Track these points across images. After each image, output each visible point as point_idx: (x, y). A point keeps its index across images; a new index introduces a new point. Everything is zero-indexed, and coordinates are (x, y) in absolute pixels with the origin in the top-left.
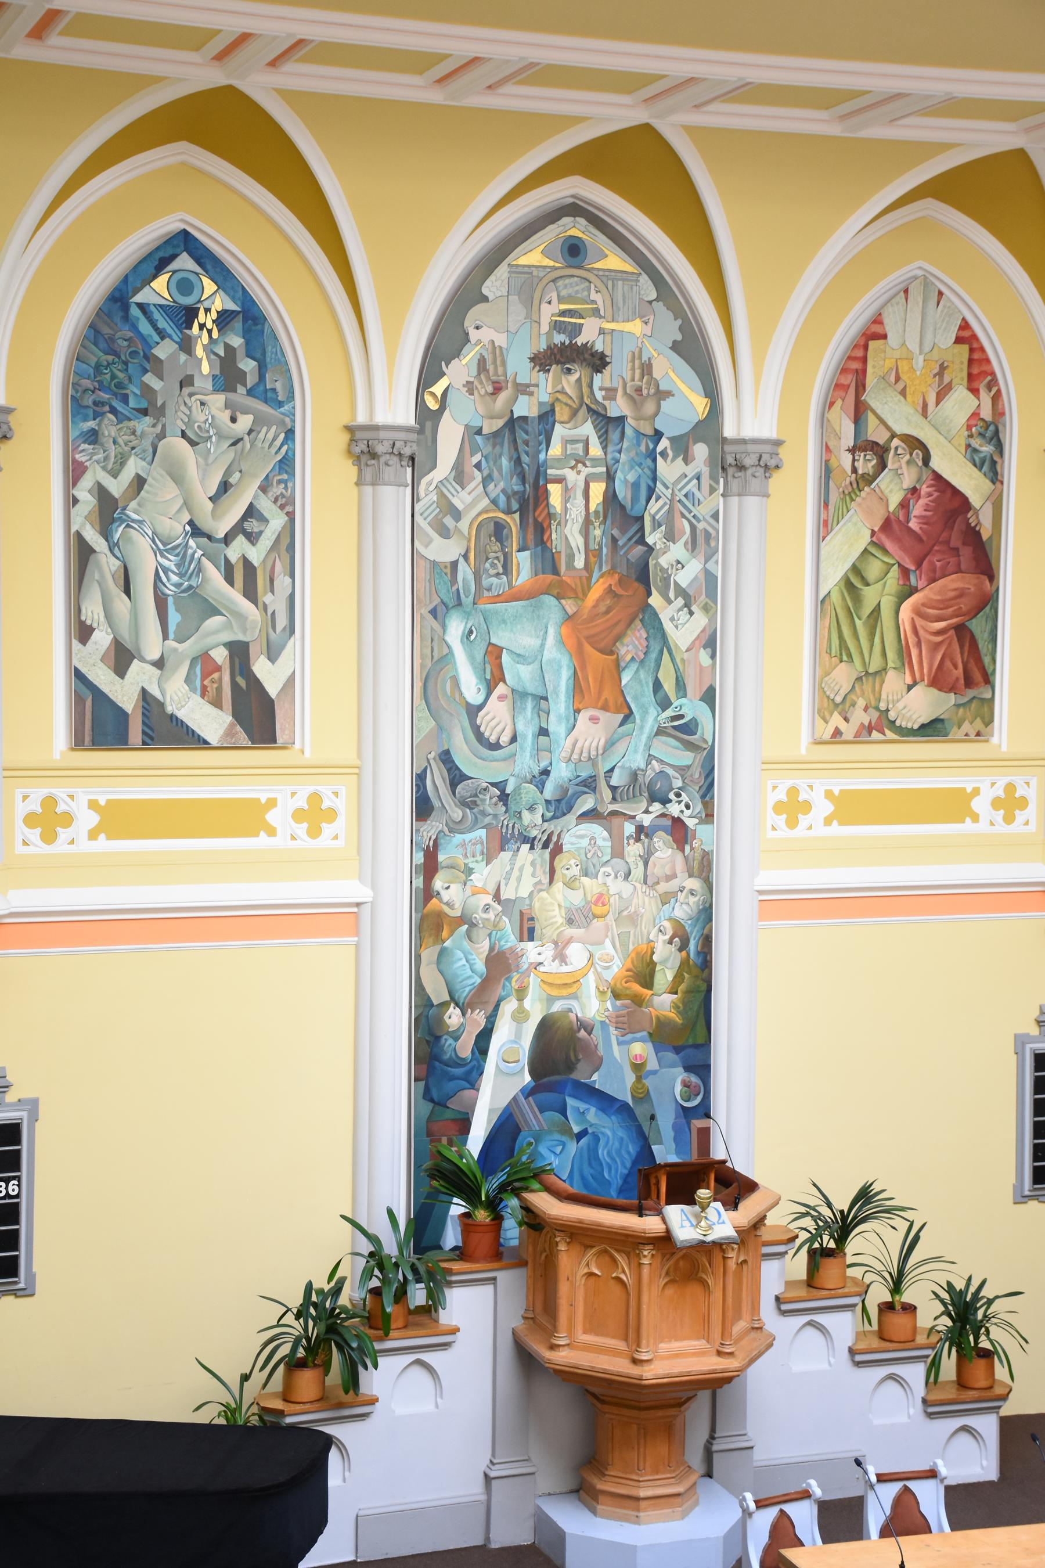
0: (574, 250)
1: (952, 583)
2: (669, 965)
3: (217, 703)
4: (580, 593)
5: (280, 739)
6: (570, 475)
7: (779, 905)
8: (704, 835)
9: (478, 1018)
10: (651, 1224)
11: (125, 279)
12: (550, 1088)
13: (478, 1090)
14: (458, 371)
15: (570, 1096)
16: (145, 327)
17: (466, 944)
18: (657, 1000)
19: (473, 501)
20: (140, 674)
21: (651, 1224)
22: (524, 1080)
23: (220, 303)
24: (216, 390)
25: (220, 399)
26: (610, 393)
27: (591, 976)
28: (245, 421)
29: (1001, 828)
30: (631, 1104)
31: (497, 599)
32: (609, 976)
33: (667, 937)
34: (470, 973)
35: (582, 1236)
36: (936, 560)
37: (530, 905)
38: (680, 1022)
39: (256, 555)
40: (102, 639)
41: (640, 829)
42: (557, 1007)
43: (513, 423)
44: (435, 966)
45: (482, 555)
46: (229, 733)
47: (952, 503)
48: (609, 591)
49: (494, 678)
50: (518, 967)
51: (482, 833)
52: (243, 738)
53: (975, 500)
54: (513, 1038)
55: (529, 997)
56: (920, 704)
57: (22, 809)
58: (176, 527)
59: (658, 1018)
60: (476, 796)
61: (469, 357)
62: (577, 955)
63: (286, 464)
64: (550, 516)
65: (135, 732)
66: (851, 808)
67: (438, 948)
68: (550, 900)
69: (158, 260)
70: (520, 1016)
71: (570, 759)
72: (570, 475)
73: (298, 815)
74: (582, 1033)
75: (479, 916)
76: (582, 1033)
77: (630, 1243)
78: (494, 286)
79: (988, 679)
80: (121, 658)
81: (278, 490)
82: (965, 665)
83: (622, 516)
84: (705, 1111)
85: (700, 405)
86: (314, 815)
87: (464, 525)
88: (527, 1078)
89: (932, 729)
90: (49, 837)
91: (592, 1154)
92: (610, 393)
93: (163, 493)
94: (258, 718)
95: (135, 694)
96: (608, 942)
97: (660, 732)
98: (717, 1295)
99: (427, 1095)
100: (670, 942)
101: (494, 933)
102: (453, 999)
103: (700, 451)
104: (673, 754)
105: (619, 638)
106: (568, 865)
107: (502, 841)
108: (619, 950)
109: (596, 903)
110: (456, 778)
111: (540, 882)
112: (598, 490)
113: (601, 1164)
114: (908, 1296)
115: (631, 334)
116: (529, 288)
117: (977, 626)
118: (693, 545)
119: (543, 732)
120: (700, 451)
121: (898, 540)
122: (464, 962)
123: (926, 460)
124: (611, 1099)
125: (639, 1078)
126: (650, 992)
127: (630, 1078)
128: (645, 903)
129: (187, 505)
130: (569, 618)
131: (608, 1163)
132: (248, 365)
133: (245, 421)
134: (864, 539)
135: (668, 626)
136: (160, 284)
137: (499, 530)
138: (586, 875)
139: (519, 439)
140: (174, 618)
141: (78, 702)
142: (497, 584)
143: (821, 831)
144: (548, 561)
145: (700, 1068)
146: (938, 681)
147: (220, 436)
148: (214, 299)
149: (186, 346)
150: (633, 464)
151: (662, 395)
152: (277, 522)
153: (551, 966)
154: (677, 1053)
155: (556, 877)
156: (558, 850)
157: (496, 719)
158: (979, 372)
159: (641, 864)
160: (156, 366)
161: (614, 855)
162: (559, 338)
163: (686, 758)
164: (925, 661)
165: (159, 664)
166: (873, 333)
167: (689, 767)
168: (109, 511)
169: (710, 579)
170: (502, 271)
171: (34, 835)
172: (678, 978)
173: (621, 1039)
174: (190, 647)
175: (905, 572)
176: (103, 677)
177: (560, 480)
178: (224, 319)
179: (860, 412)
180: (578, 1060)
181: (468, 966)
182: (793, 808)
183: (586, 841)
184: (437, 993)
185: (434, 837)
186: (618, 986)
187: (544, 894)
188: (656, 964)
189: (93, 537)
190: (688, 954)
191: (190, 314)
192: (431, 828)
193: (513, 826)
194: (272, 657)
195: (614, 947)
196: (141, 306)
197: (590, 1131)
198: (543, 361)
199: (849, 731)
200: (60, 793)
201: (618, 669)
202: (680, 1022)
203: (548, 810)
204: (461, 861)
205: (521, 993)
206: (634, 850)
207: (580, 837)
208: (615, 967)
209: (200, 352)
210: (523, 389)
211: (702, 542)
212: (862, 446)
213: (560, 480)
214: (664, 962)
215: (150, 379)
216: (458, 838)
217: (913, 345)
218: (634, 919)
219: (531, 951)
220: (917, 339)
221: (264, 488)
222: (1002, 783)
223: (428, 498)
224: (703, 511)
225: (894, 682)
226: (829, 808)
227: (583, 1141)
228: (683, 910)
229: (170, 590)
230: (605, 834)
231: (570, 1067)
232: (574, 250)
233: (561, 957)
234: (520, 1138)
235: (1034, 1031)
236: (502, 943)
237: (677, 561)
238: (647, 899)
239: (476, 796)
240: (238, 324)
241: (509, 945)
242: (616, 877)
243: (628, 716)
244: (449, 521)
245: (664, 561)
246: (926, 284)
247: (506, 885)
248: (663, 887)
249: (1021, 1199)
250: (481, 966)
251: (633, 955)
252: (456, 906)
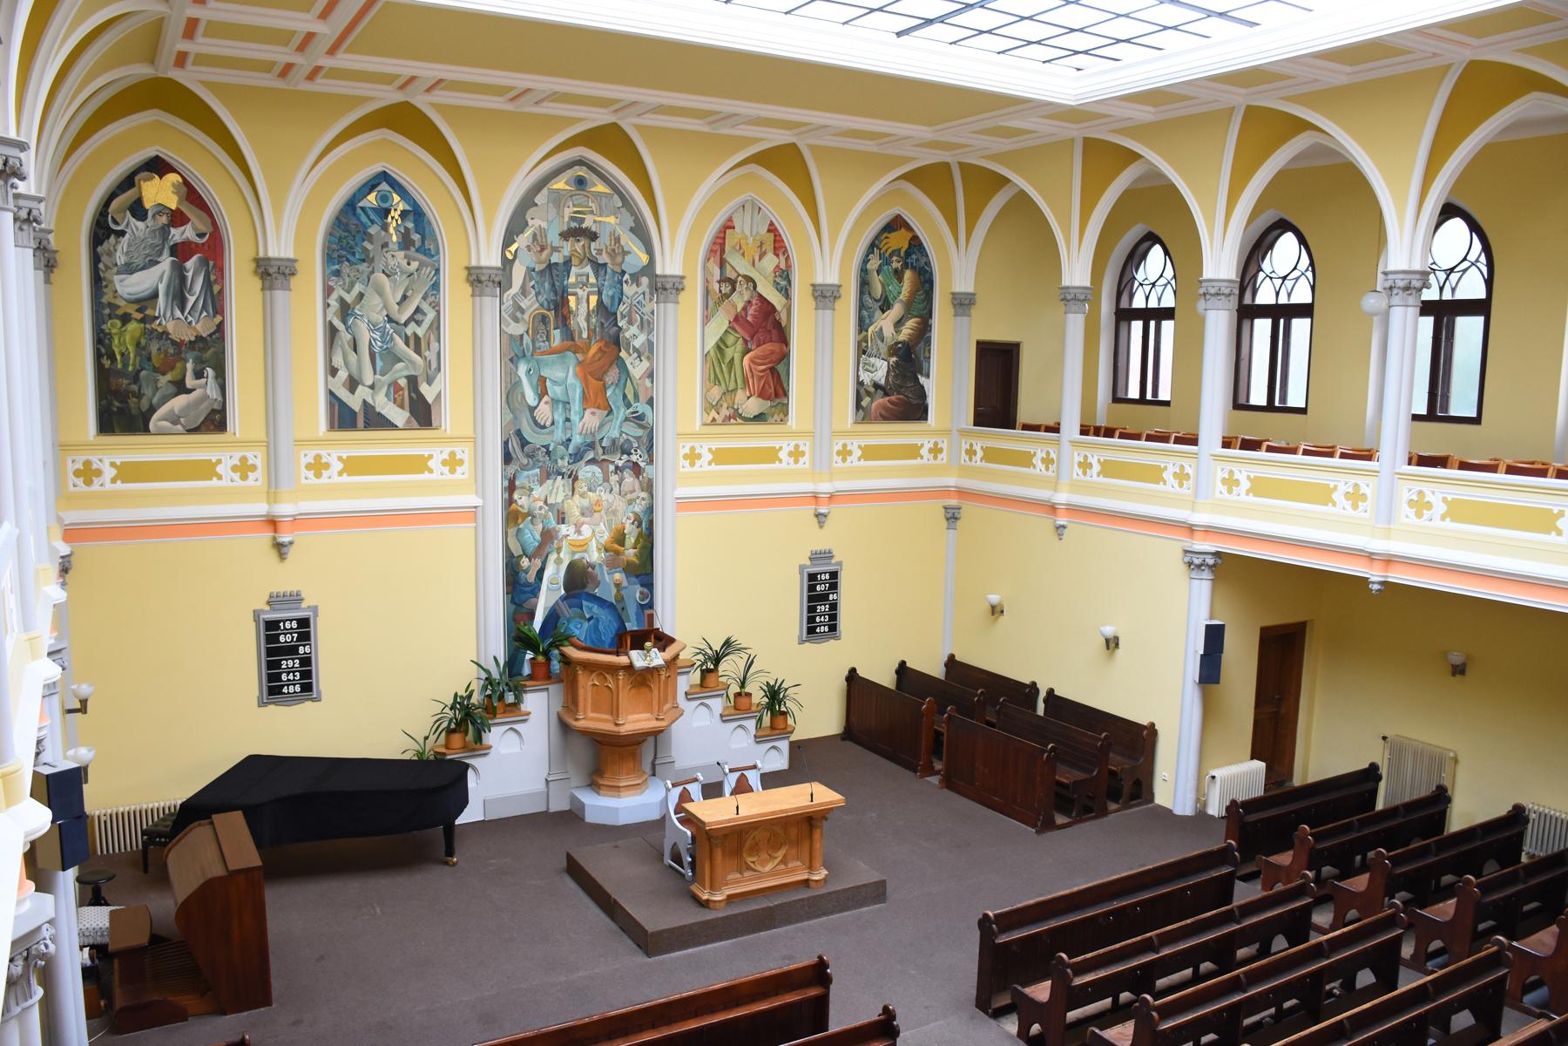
0: (580, 182)
1: (768, 347)
3: (402, 407)
4: (583, 349)
5: (434, 424)
6: (580, 291)
7: (687, 505)
8: (649, 471)
10: (623, 660)
11: (354, 195)
12: (574, 596)
14: (523, 240)
16: (364, 218)
19: (530, 304)
20: (362, 392)
21: (623, 660)
23: (401, 207)
24: (400, 249)
25: (402, 253)
26: (600, 252)
28: (415, 265)
29: (792, 466)
31: (542, 354)
32: (602, 541)
35: (589, 666)
36: (760, 336)
39: (420, 332)
40: (343, 374)
41: (617, 468)
42: (577, 556)
43: (551, 266)
45: (536, 332)
46: (408, 422)
47: (767, 308)
48: (600, 349)
49: (542, 392)
52: (415, 424)
53: (779, 307)
56: (753, 406)
57: (304, 461)
58: (380, 318)
61: (528, 233)
62: (586, 530)
63: (436, 286)
64: (570, 312)
65: (360, 421)
66: (720, 457)
69: (371, 185)
70: (559, 561)
72: (580, 291)
73: (444, 463)
75: (537, 512)
77: (613, 669)
78: (541, 199)
79: (786, 394)
80: (353, 384)
81: (431, 299)
82: (774, 387)
83: (606, 312)
84: (651, 605)
85: (644, 258)
86: (452, 463)
87: (526, 317)
89: (760, 418)
90: (318, 475)
91: (596, 629)
92: (600, 252)
93: (373, 301)
94: (423, 414)
95: (360, 402)
97: (626, 419)
98: (656, 692)
99: (513, 601)
103: (645, 280)
104: (633, 431)
105: (605, 373)
106: (582, 486)
107: (547, 475)
110: (524, 443)
112: (594, 299)
114: (747, 690)
115: (609, 223)
116: (558, 199)
117: (780, 368)
118: (641, 327)
119: (568, 420)
120: (645, 280)
121: (742, 326)
123: (755, 287)
127: (614, 591)
128: (620, 504)
129: (385, 307)
130: (580, 363)
132: (416, 237)
133: (415, 265)
134: (726, 325)
135: (630, 367)
136: (372, 197)
137: (544, 319)
139: (554, 274)
140: (379, 364)
141: (331, 407)
142: (543, 346)
143: (706, 468)
144: (569, 335)
145: (648, 584)
146: (762, 395)
147: (402, 272)
148: (398, 204)
149: (385, 227)
150: (611, 287)
151: (625, 253)
152: (431, 315)
153: (573, 536)
156: (576, 479)
157: (544, 412)
158: (779, 246)
160: (370, 238)
162: (574, 225)
163: (639, 432)
164: (755, 384)
165: (372, 387)
166: (728, 226)
168: (345, 310)
169: (650, 344)
170: (545, 191)
171: (311, 474)
172: (637, 541)
174: (387, 378)
175: (745, 341)
176: (343, 394)
177: (575, 294)
178: (404, 214)
179: (722, 264)
182: (693, 457)
184: (517, 551)
189: (337, 323)
191: (388, 211)
192: (511, 469)
194: (430, 383)
196: (363, 209)
198: (565, 235)
199: (719, 419)
200: (323, 453)
201: (605, 388)
205: (559, 550)
206: (614, 478)
207: (587, 472)
208: (606, 537)
209: (391, 230)
210: (555, 249)
211: (646, 325)
212: (724, 280)
213: (575, 294)
215: (367, 244)
217: (748, 233)
218: (614, 513)
219: (563, 529)
220: (748, 230)
221: (424, 298)
222: (793, 444)
223: (508, 303)
224: (646, 310)
225: (741, 395)
226: (710, 457)
228: (639, 508)
229: (377, 350)
231: (584, 586)
232: (580, 182)
233: (579, 532)
235: (808, 563)
237: (634, 335)
240: (411, 217)
243: (610, 412)
244: (518, 314)
245: (627, 335)
246: (753, 204)
248: (629, 496)
249: (802, 642)
250: (538, 537)
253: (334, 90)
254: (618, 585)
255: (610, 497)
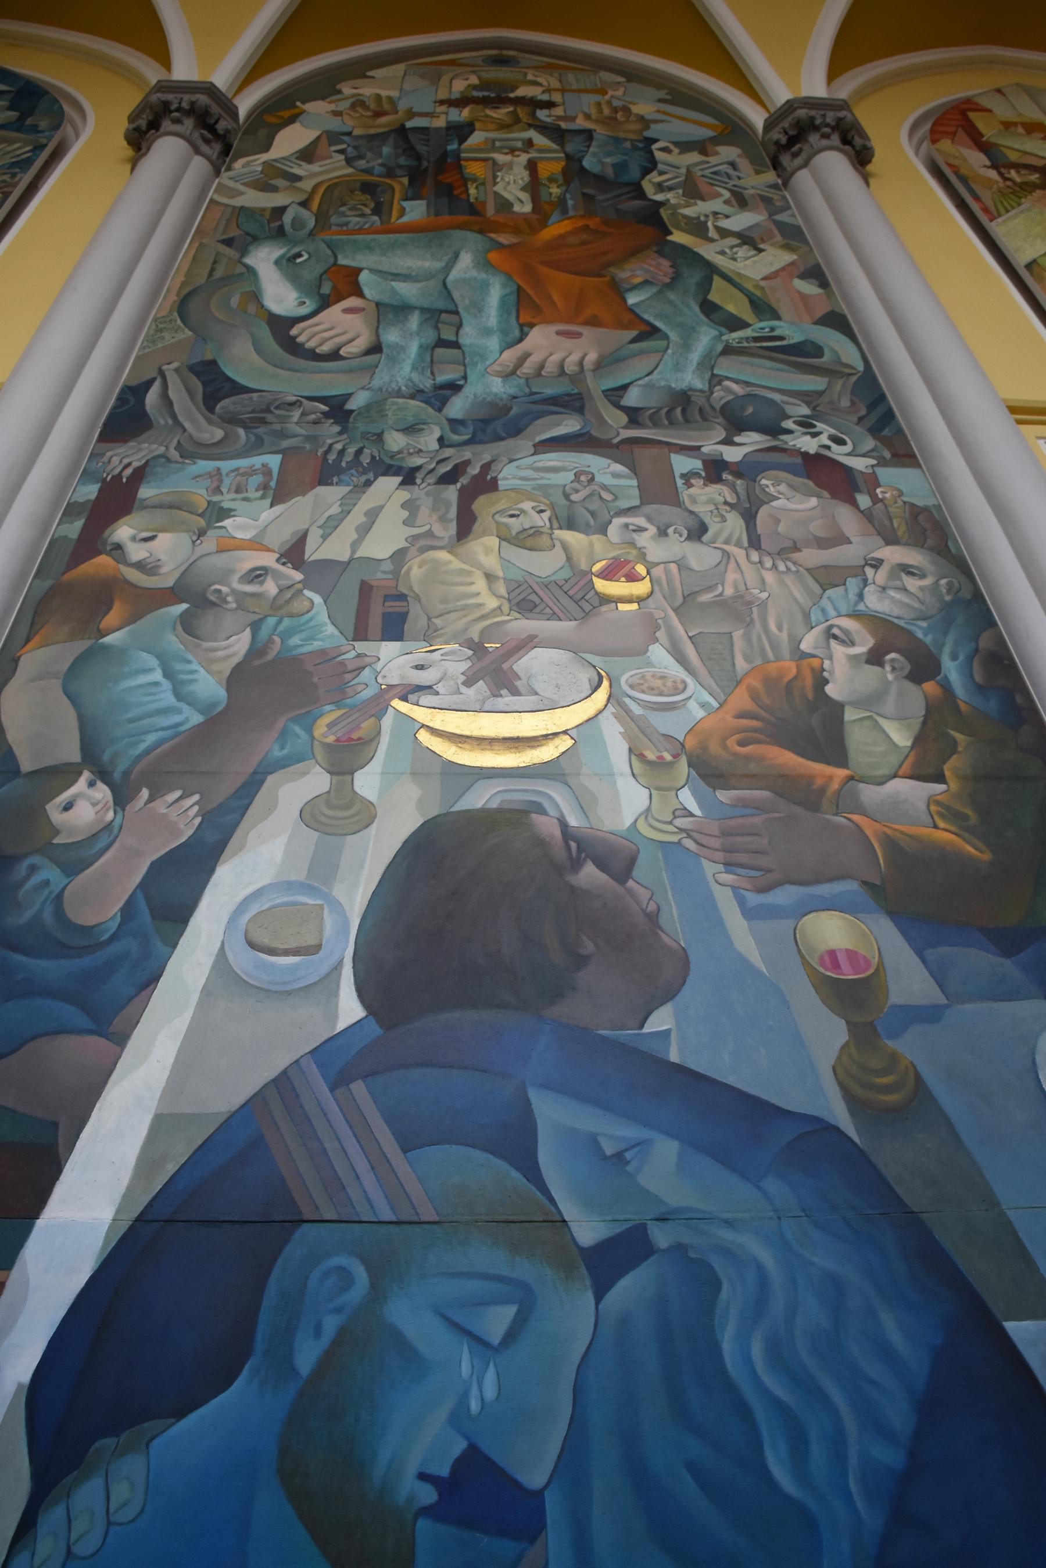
2: (890, 705)
6: (501, 158)
9: (173, 813)
13: (121, 1040)
15: (546, 1086)
17: (173, 641)
18: (869, 793)
22: (333, 1016)
27: (612, 732)
30: (841, 1116)
32: (675, 726)
33: (860, 650)
34: (167, 698)
37: (396, 573)
38: (987, 856)
42: (479, 798)
44: (56, 684)
50: (339, 694)
51: (274, 461)
54: (299, 875)
55: (376, 765)
59: (891, 844)
60: (268, 410)
67: (81, 646)
68: (456, 564)
70: (338, 816)
71: (513, 373)
74: (590, 874)
76: (590, 874)
88: (350, 1009)
96: (659, 654)
100: (875, 658)
101: (272, 621)
102: (95, 761)
108: (702, 671)
109: (607, 574)
111: (430, 534)
113: (743, 1411)
122: (157, 676)
124: (757, 1112)
125: (864, 1035)
126: (842, 773)
127: (827, 1034)
131: (778, 1404)
138: (571, 525)
154: (1007, 953)
155: (477, 527)
159: (735, 523)
161: (647, 496)
167: (820, 393)
173: (753, 899)
180: (581, 961)
181: (166, 684)
183: (571, 476)
185: (136, 464)
186: (715, 748)
187: (443, 555)
188: (840, 707)
190: (947, 688)
193: (359, 452)
195: (682, 660)
197: (661, 1237)
202: (987, 856)
203: (454, 431)
204: (200, 495)
205: (347, 756)
206: (704, 497)
208: (698, 706)
214: (869, 701)
216: (205, 466)
218: (740, 609)
219: (392, 660)
227: (630, 1288)
230: (618, 468)
234: (295, 1250)
236: (295, 640)
238: (769, 577)
239: (268, 410)
241: (317, 645)
242: (663, 533)
247: (325, 537)
248: (812, 557)
250: (209, 687)
251: (755, 683)
252: (164, 570)
253: (8, 201)
254: (851, 993)
255: (701, 557)
